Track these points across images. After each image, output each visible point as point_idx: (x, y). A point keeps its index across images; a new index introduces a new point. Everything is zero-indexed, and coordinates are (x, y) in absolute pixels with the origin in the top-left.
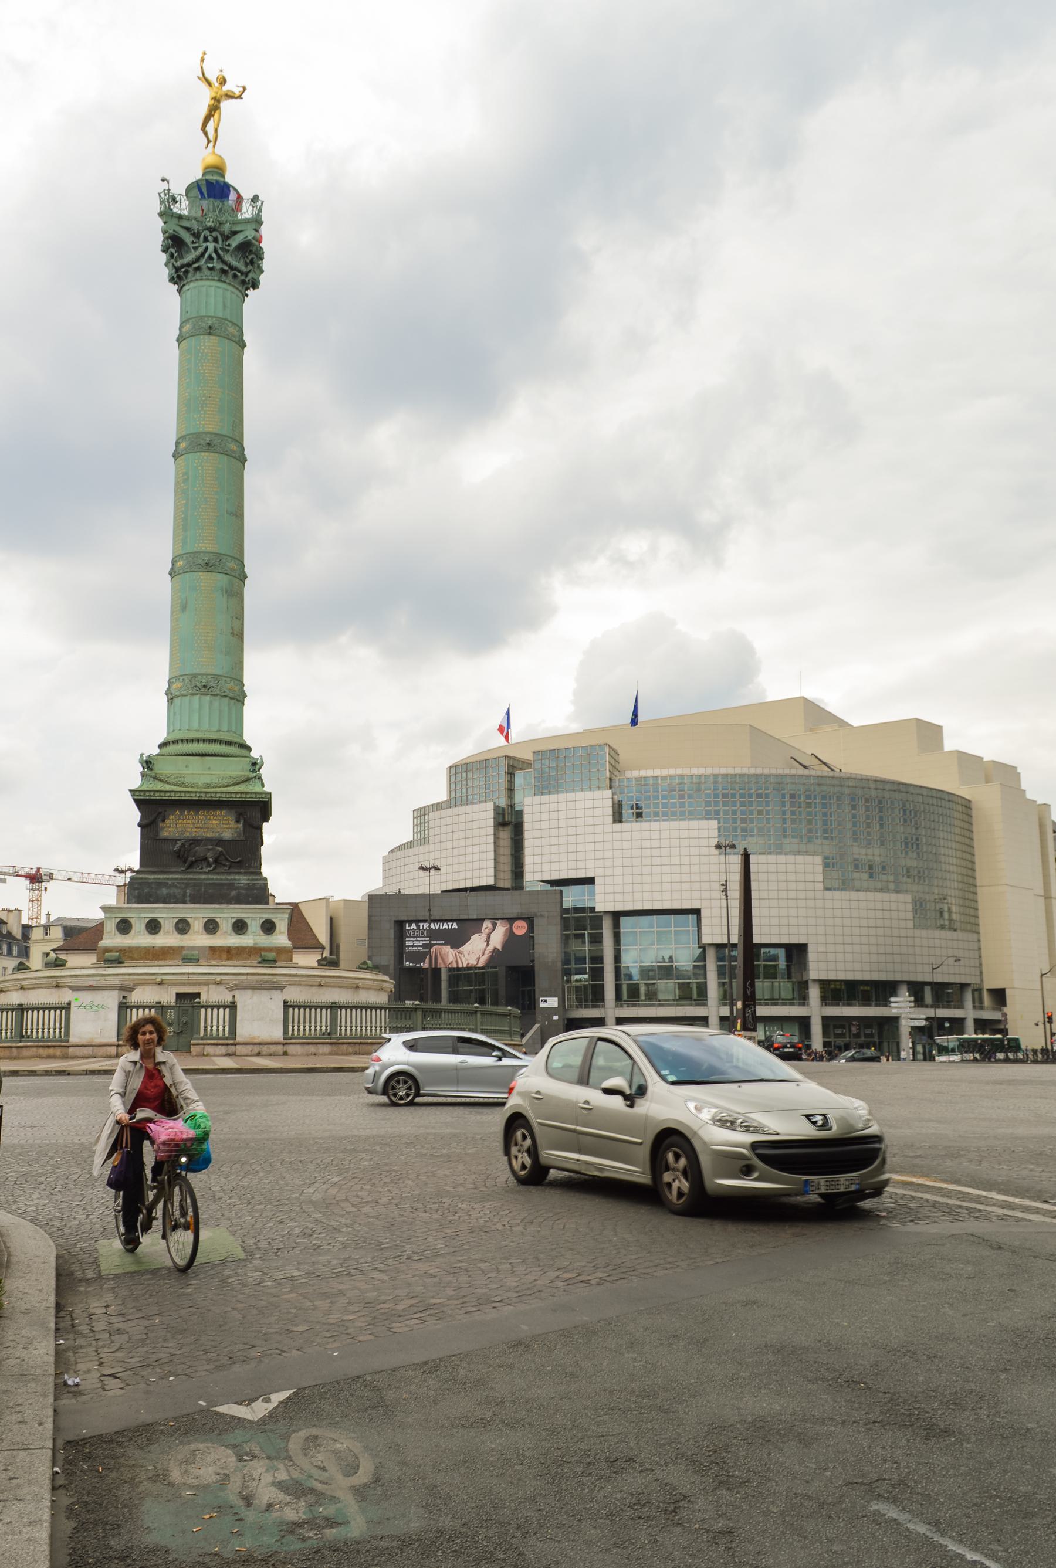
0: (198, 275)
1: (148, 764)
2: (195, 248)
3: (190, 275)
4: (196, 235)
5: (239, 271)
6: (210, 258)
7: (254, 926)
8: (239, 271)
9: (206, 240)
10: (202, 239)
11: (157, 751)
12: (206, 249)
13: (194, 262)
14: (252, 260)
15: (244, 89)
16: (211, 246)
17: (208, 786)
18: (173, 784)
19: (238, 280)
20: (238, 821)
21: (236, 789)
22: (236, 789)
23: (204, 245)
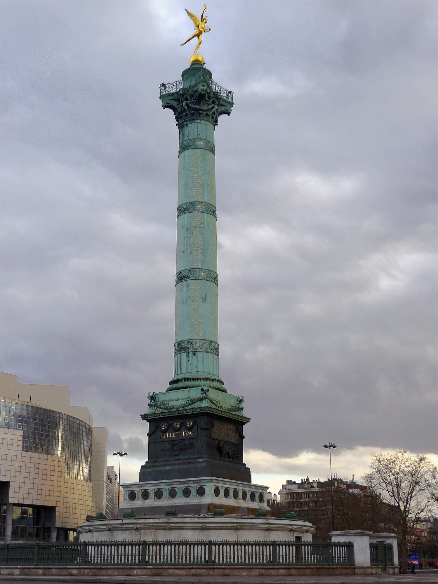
0: (206, 118)
3: (201, 116)
4: (209, 97)
6: (214, 113)
9: (214, 102)
10: (211, 101)
12: (213, 107)
13: (206, 111)
15: (210, 30)
20: (236, 433)
23: (213, 105)
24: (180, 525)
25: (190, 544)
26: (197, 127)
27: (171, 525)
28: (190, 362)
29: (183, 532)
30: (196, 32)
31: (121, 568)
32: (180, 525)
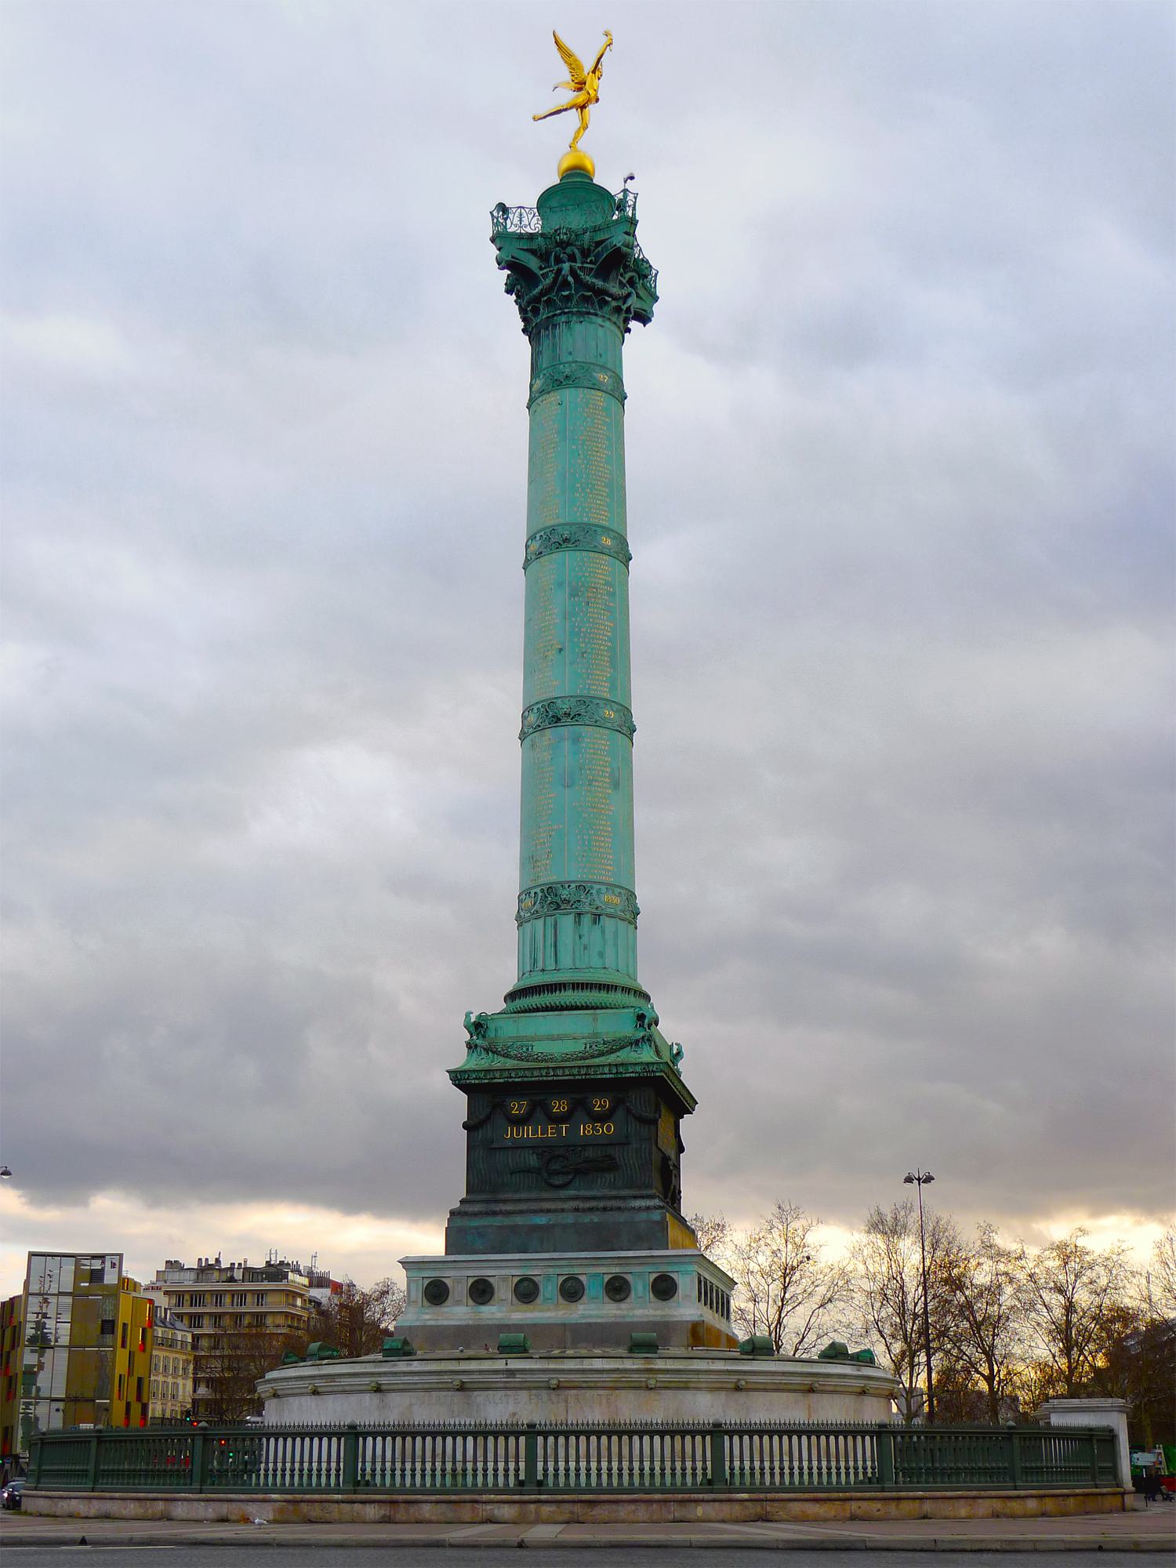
1: (478, 1027)
2: (545, 276)
4: (543, 256)
5: (610, 295)
7: (640, 1287)
8: (610, 295)
9: (558, 260)
11: (502, 1006)
12: (560, 270)
14: (631, 278)
16: (566, 266)
17: (567, 1057)
18: (515, 1057)
19: (606, 309)
21: (612, 1058)
22: (612, 1058)
24: (684, 1378)
25: (631, 1434)
26: (581, 336)
27: (661, 1377)
28: (585, 940)
29: (688, 1396)
30: (568, 96)
31: (658, 1501)
32: (684, 1378)
